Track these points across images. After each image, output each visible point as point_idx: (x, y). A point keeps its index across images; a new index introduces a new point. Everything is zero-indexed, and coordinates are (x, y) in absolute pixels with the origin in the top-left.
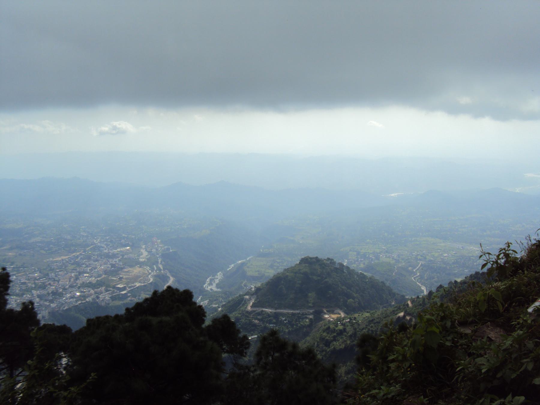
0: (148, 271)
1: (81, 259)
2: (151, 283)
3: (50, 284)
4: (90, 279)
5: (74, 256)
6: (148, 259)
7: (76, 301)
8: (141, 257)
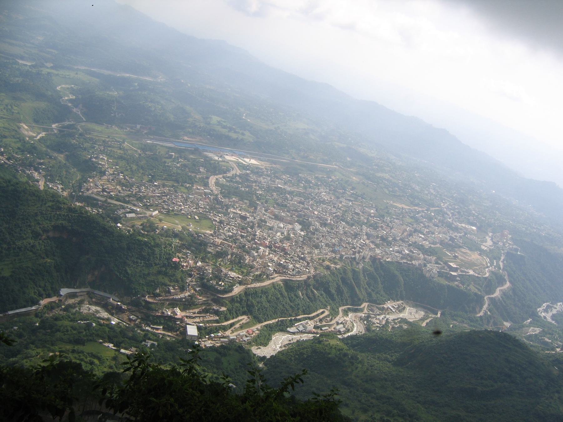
0: (487, 264)
1: (422, 216)
2: (486, 278)
3: (382, 227)
5: (416, 210)
6: (490, 250)
7: (402, 258)
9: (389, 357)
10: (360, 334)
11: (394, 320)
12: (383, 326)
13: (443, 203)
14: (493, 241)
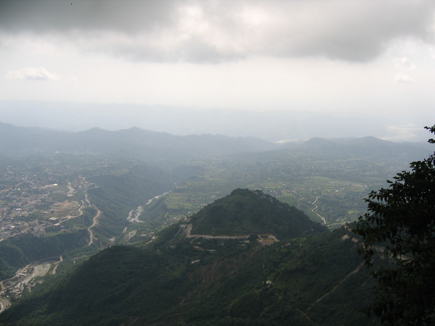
0: (78, 206)
1: (11, 194)
2: (82, 216)
4: (23, 213)
5: (4, 192)
6: (75, 194)
7: (12, 233)
8: (68, 193)
9: (40, 311)
10: (8, 307)
11: (29, 282)
12: (24, 291)
13: (23, 177)
14: (74, 188)
